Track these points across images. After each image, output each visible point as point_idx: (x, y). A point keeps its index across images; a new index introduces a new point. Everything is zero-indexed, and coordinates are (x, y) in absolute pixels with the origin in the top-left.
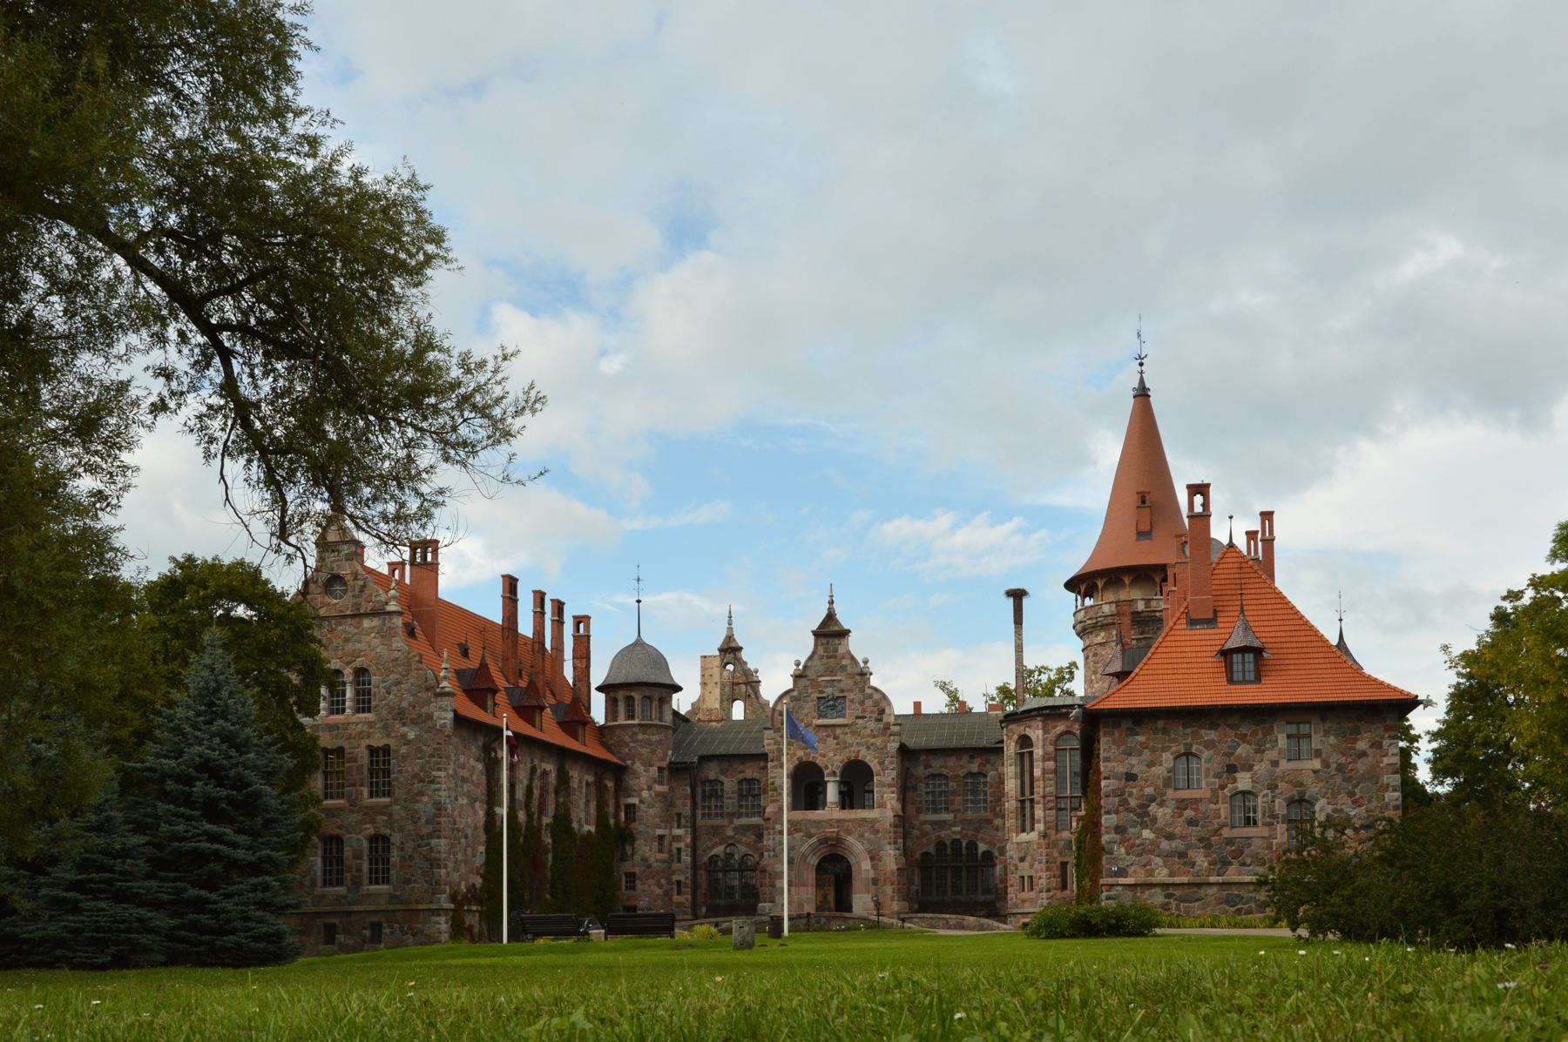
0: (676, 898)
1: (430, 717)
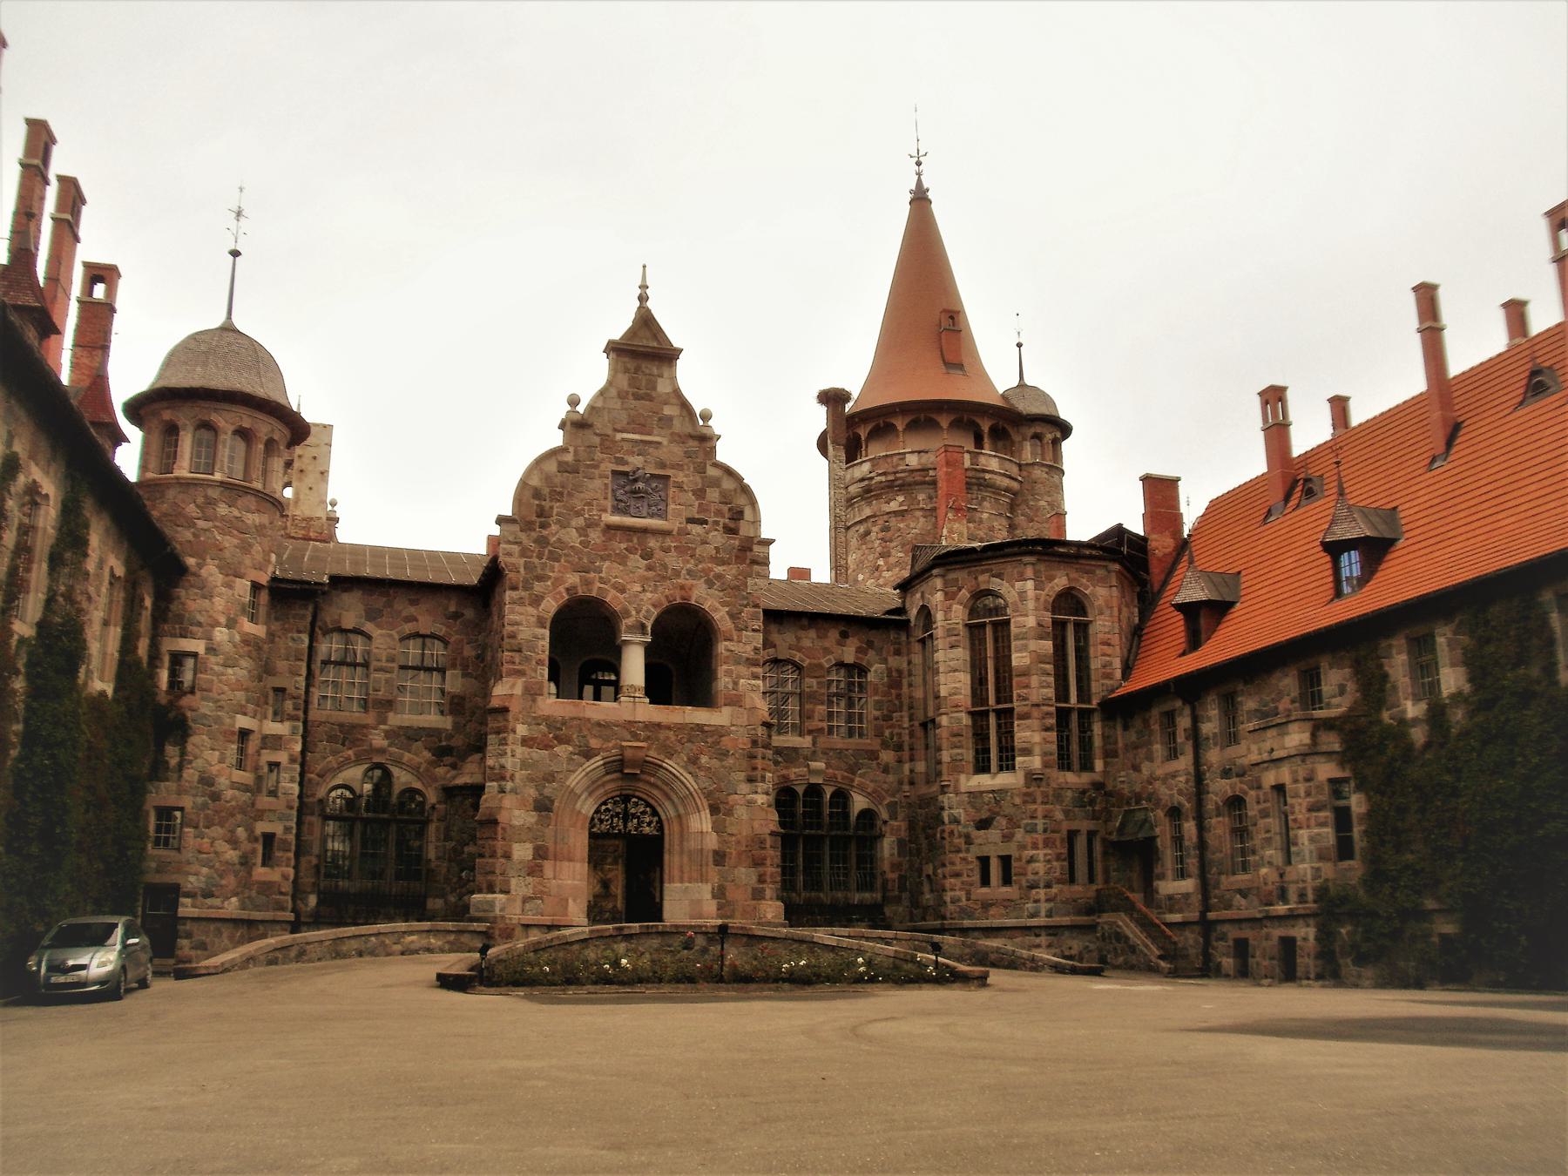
0: (261, 873)
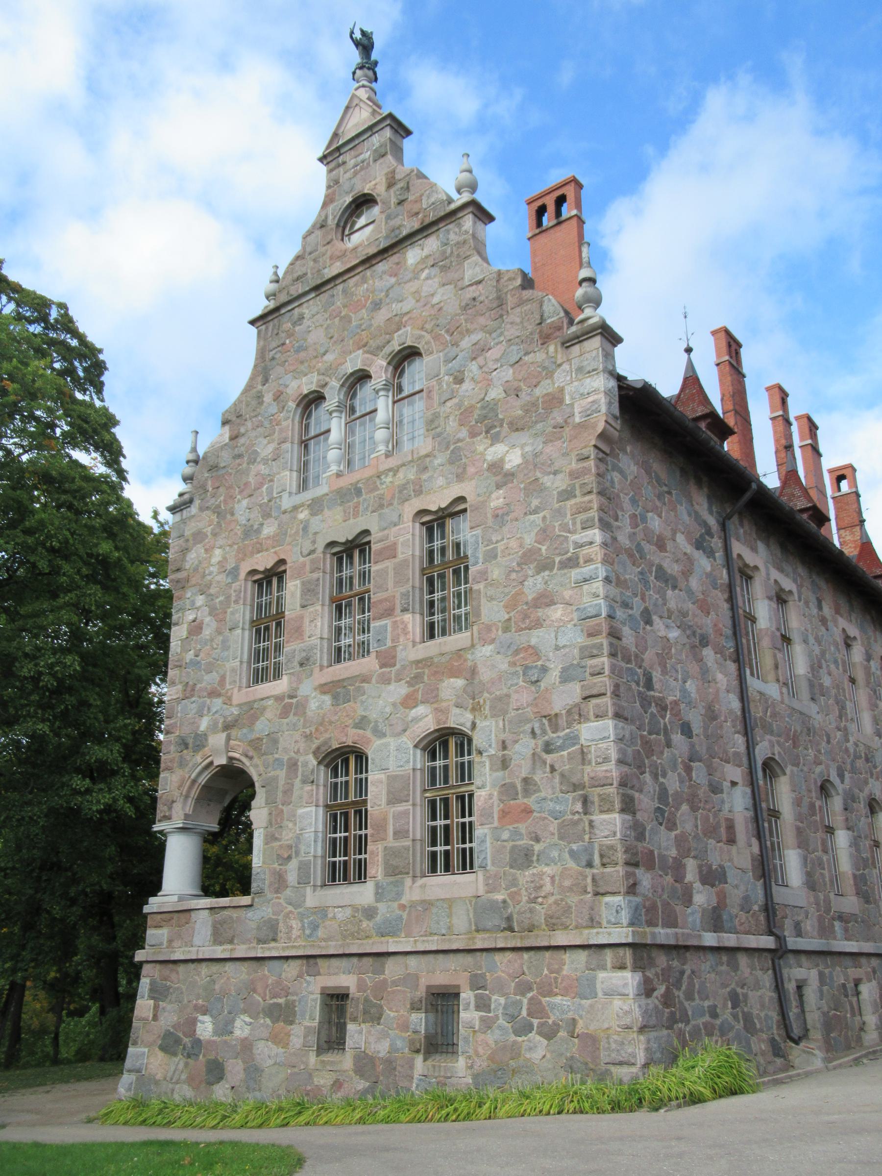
1: (555, 400)
